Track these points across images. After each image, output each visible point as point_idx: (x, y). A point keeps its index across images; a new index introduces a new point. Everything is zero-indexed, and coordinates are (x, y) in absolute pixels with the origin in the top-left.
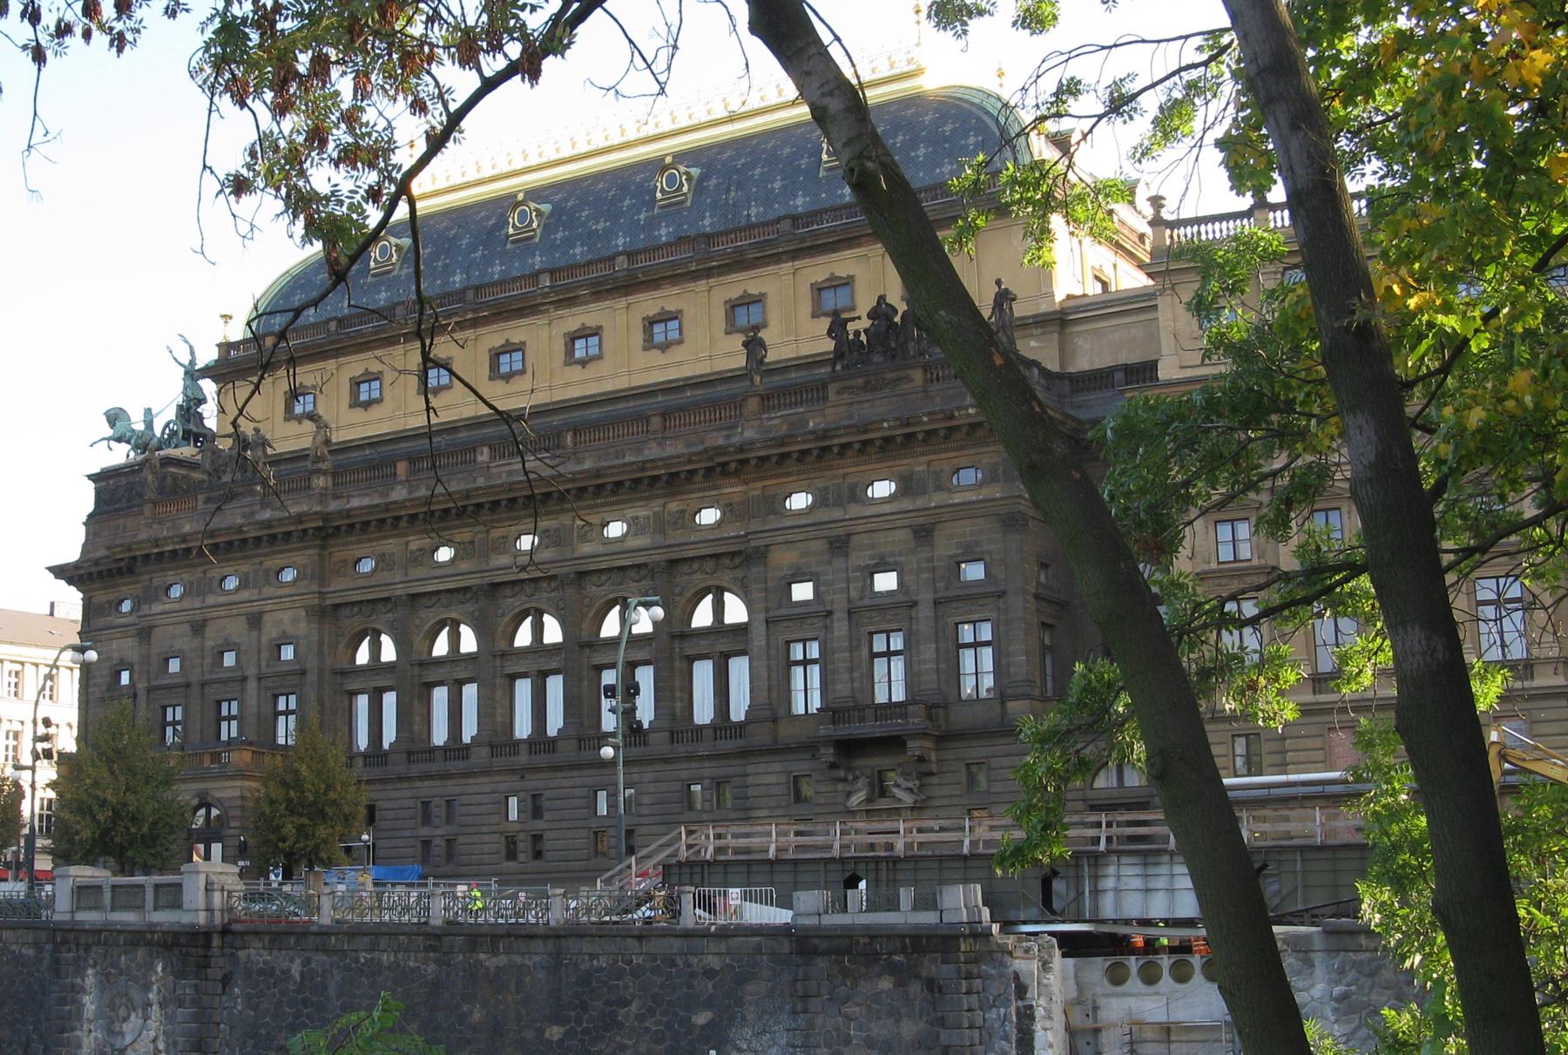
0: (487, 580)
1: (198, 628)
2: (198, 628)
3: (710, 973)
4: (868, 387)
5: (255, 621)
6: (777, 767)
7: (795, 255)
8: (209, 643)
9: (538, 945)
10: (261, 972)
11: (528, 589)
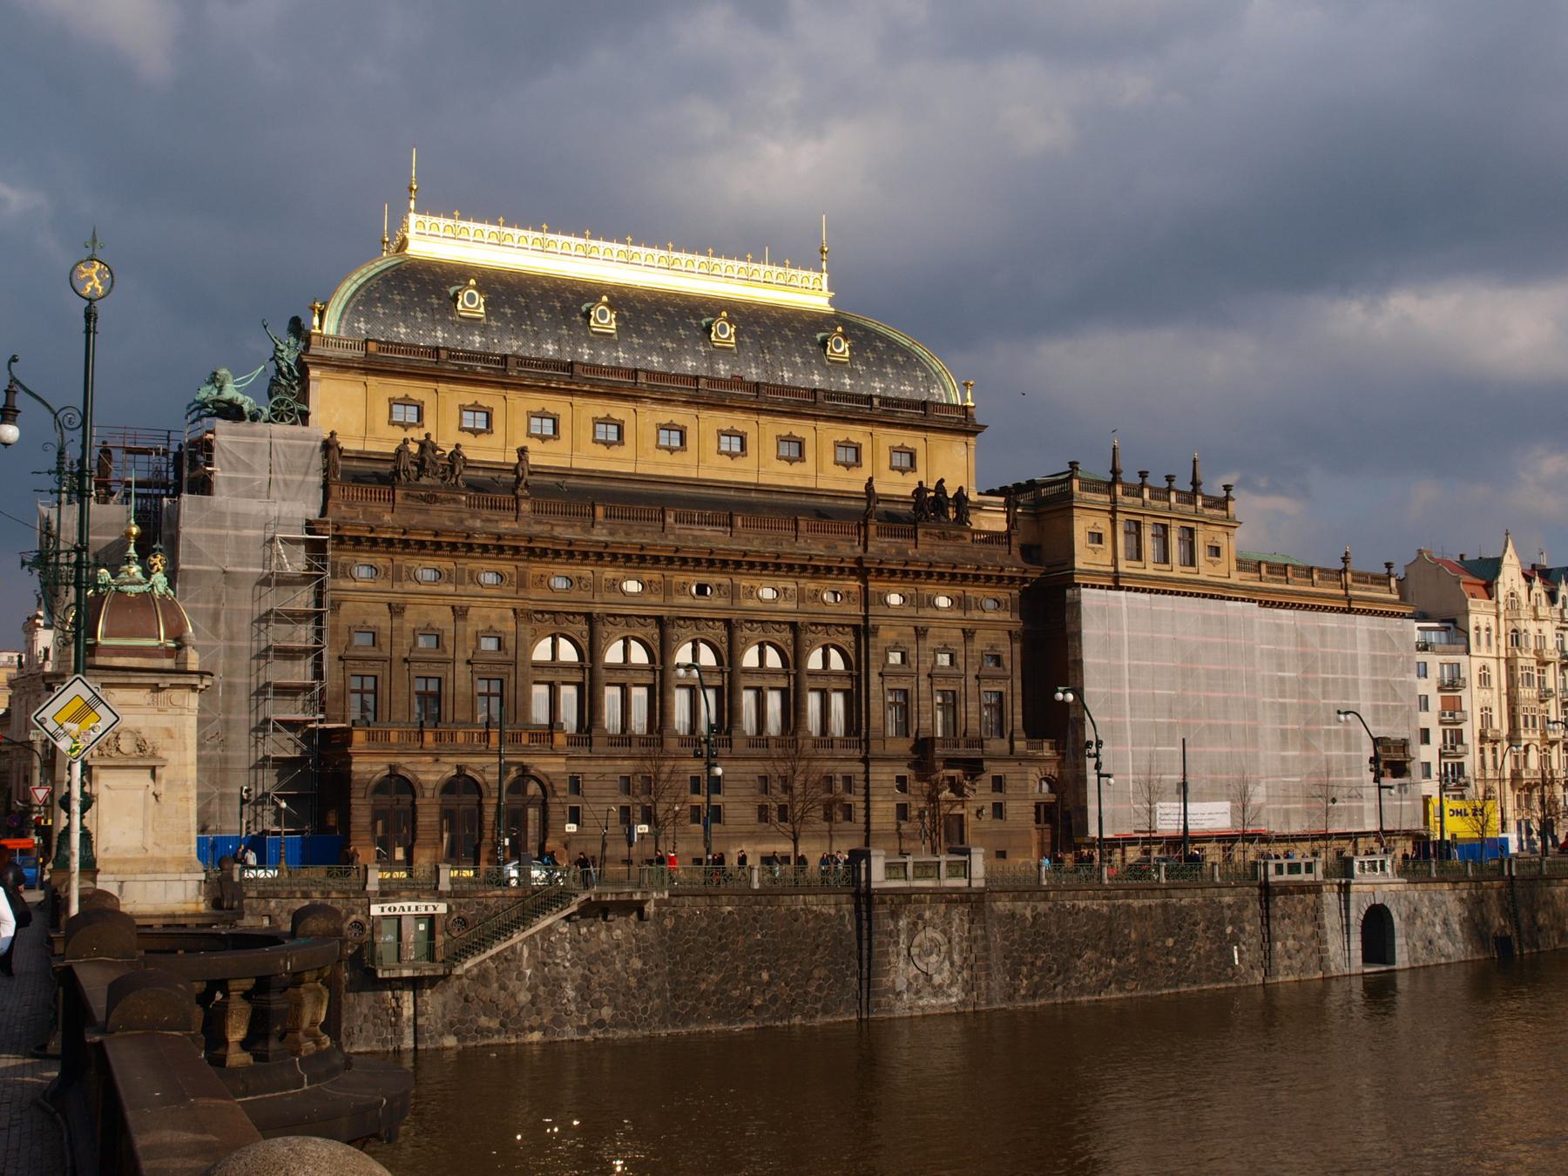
0: (675, 612)
1: (396, 610)
2: (396, 610)
3: (1229, 906)
4: (943, 536)
5: (460, 613)
6: (888, 770)
7: (828, 419)
8: (409, 626)
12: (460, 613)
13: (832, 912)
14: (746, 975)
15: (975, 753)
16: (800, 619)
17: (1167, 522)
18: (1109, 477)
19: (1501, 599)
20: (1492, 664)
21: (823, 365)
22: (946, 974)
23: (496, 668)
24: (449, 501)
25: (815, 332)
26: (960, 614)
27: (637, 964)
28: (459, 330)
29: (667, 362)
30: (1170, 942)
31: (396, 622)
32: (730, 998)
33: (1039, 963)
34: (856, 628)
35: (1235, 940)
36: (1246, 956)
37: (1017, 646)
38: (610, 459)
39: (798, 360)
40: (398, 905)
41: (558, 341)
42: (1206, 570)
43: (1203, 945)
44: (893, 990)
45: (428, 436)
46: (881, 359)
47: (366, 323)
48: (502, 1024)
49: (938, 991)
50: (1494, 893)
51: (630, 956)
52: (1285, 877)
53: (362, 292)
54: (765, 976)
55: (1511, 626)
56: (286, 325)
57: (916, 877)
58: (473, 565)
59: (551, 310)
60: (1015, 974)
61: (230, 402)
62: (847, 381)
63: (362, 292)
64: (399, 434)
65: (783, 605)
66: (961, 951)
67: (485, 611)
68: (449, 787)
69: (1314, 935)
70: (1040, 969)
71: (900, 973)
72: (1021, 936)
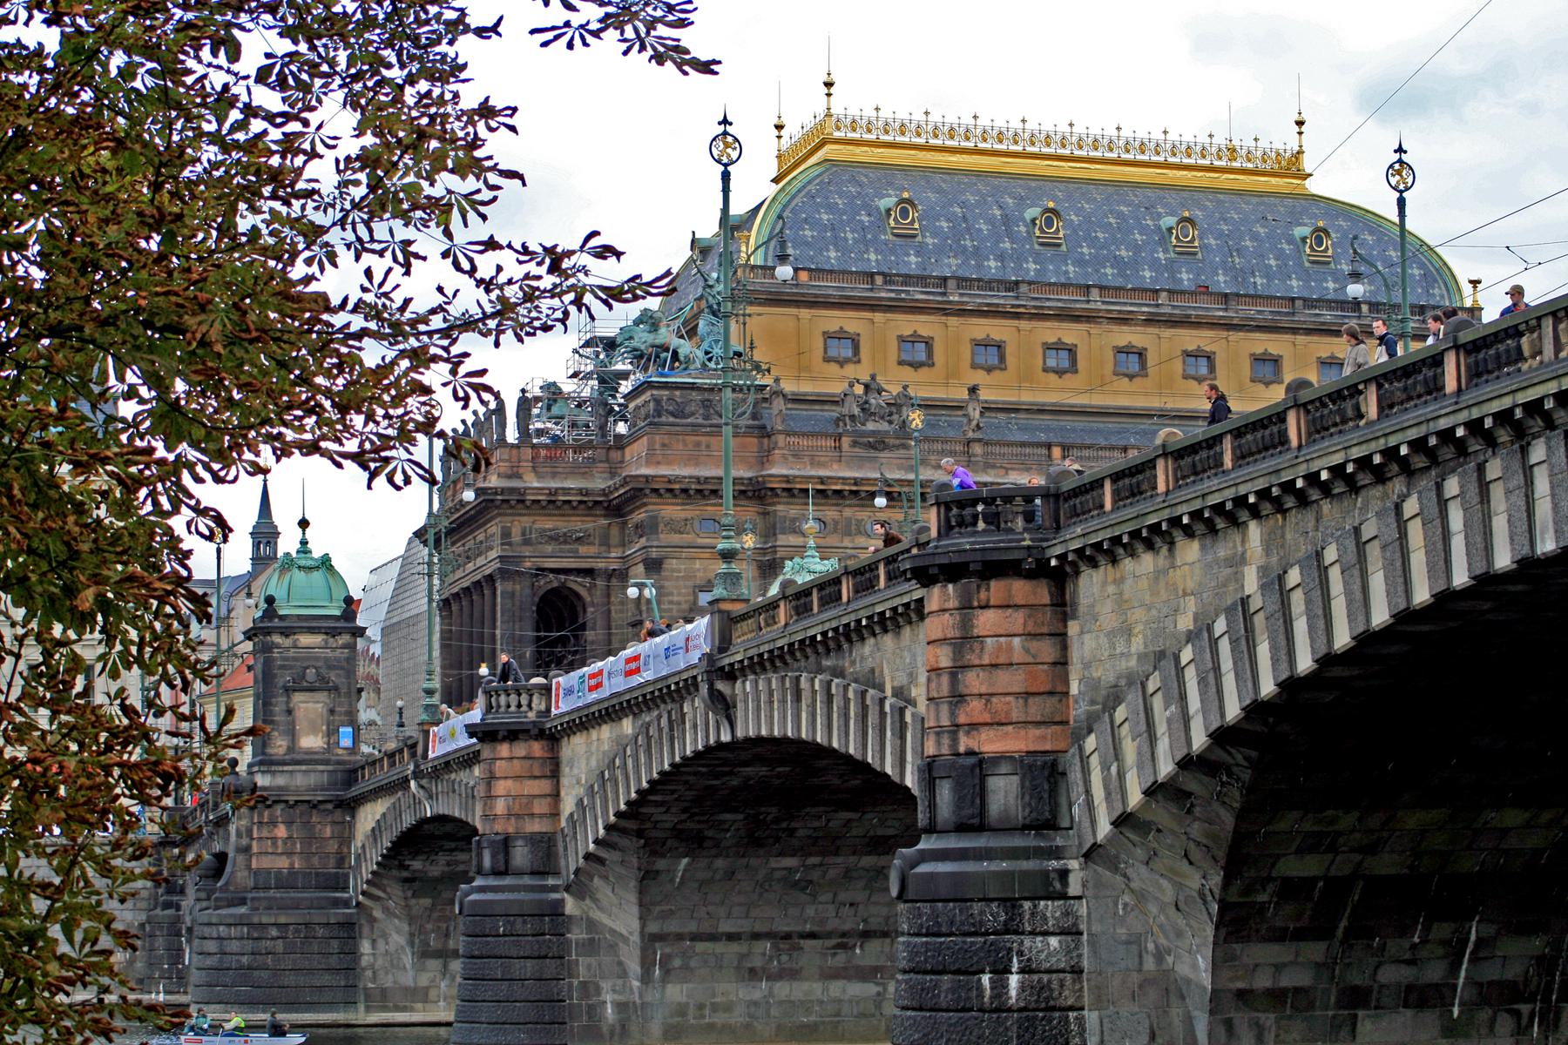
24: (898, 447)
28: (893, 251)
29: (1122, 274)
38: (1062, 390)
39: (1273, 262)
41: (1001, 257)
59: (991, 221)
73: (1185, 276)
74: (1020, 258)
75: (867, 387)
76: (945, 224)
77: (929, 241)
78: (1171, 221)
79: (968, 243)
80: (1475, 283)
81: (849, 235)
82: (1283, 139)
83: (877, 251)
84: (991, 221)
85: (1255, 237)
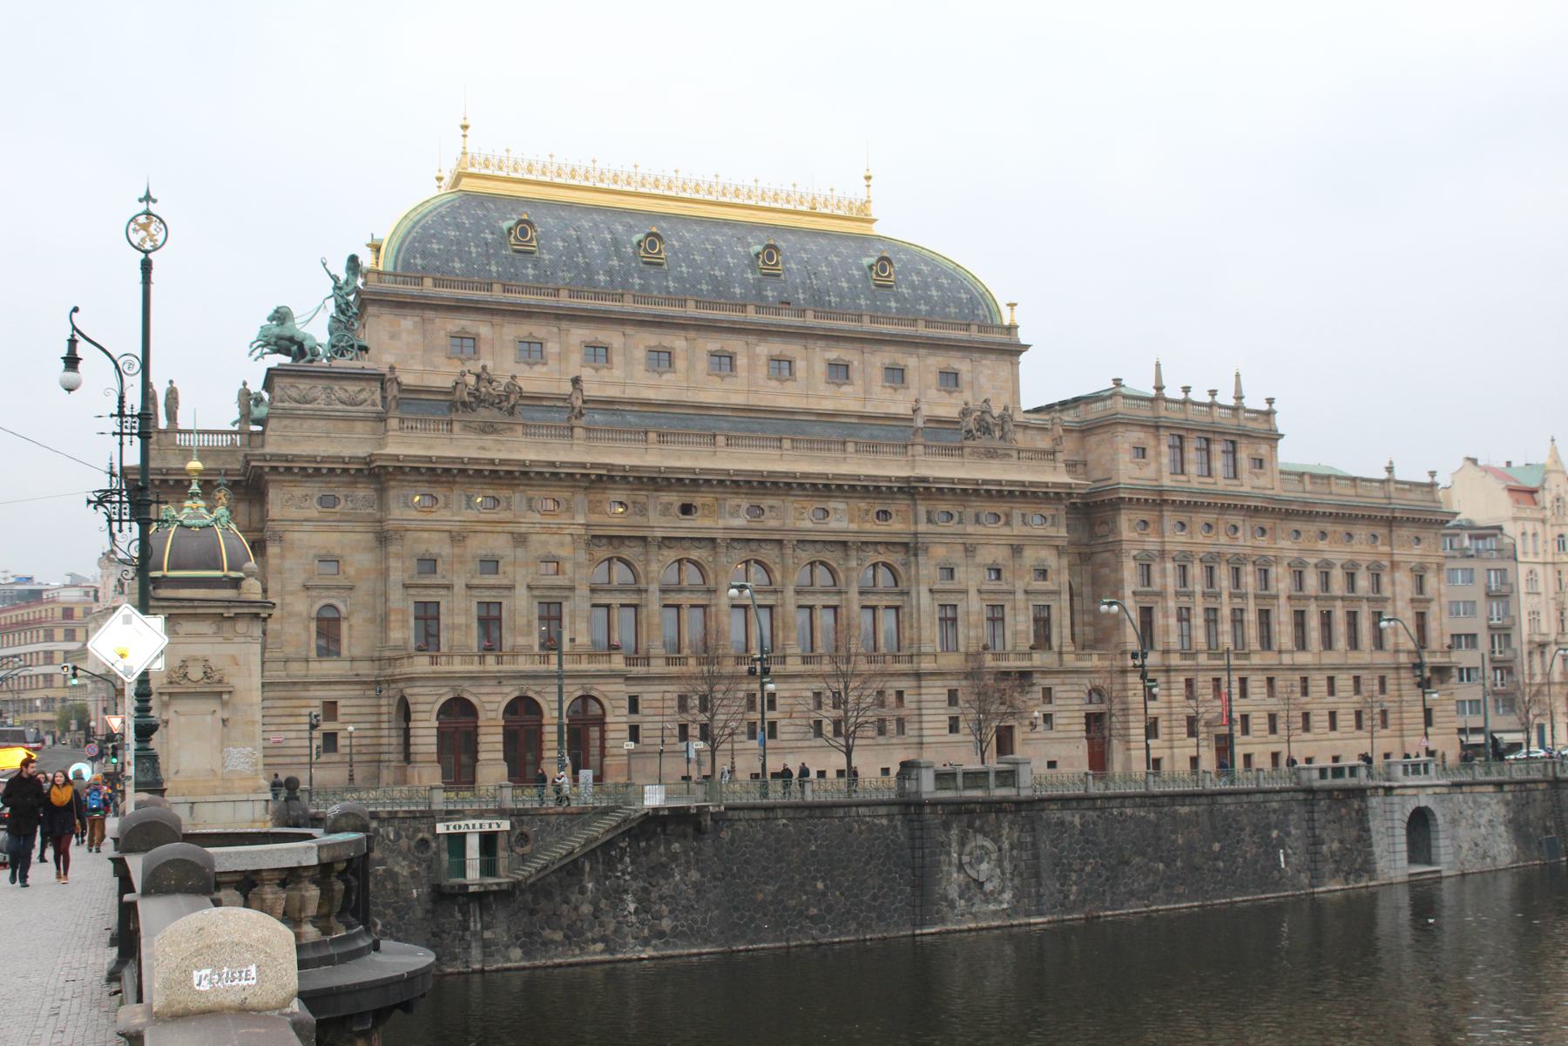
1: (457, 538)
3: (1275, 811)
6: (939, 683)
9: (1204, 800)
10: (1056, 824)
11: (754, 546)
12: (520, 540)
13: (885, 822)
14: (802, 885)
15: (1024, 664)
16: (849, 538)
17: (1210, 436)
18: (1153, 393)
19: (1548, 505)
20: (1539, 569)
21: (869, 288)
22: (996, 882)
23: (554, 593)
25: (859, 257)
26: (1006, 531)
27: (695, 875)
28: (513, 264)
30: (1216, 847)
31: (457, 551)
32: (786, 908)
33: (1088, 869)
34: (906, 545)
35: (1281, 844)
36: (1293, 860)
37: (1065, 562)
39: (845, 285)
40: (462, 823)
41: (610, 272)
42: (1249, 484)
43: (1250, 849)
44: (945, 898)
45: (484, 368)
46: (925, 282)
47: (423, 258)
48: (566, 937)
49: (988, 897)
50: (1539, 796)
51: (689, 869)
52: (1330, 782)
53: (417, 228)
54: (820, 885)
55: (1557, 531)
56: (344, 263)
57: (966, 788)
58: (530, 493)
59: (603, 243)
60: (1064, 879)
61: (291, 340)
62: (893, 304)
63: (417, 228)
64: (456, 367)
65: (834, 524)
66: (1012, 858)
67: (543, 537)
68: (513, 708)
69: (1359, 839)
70: (1089, 875)
71: (952, 882)
72: (1070, 844)
73: (769, 294)
74: (628, 274)
75: (478, 377)
76: (560, 244)
77: (546, 257)
78: (759, 248)
79: (580, 260)
80: (1012, 305)
81: (473, 250)
82: (853, 191)
83: (497, 264)
84: (603, 243)
85: (830, 264)
